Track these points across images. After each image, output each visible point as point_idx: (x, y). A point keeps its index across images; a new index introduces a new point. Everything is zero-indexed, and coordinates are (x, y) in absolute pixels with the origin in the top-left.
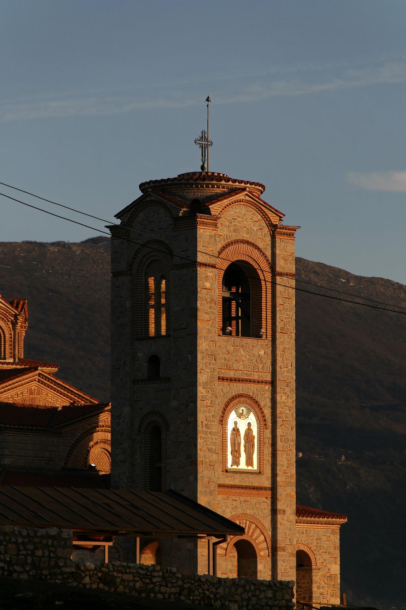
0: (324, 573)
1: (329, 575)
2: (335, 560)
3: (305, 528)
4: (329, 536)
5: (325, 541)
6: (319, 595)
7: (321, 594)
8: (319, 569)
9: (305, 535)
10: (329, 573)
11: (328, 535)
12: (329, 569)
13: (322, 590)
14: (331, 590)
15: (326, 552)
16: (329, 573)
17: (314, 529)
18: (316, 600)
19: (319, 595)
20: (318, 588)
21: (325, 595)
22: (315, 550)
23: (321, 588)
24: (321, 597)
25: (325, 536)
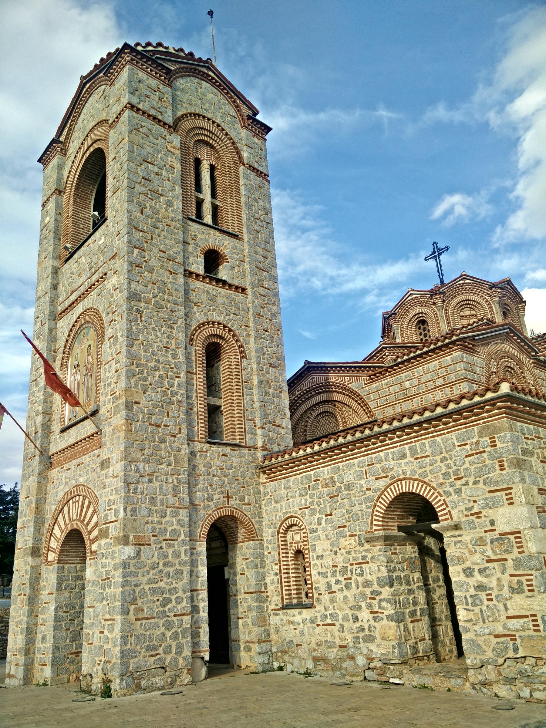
0: (479, 532)
1: (495, 535)
2: (506, 494)
3: (407, 444)
4: (477, 443)
5: (467, 456)
6: (472, 591)
7: (480, 587)
8: (457, 527)
9: (409, 459)
10: (495, 530)
11: (474, 440)
12: (492, 523)
13: (478, 578)
14: (511, 575)
15: (475, 483)
16: (495, 530)
17: (430, 439)
18: (467, 604)
19: (472, 591)
20: (469, 572)
21: (491, 589)
22: (442, 484)
23: (476, 573)
24: (483, 595)
25: (466, 444)
